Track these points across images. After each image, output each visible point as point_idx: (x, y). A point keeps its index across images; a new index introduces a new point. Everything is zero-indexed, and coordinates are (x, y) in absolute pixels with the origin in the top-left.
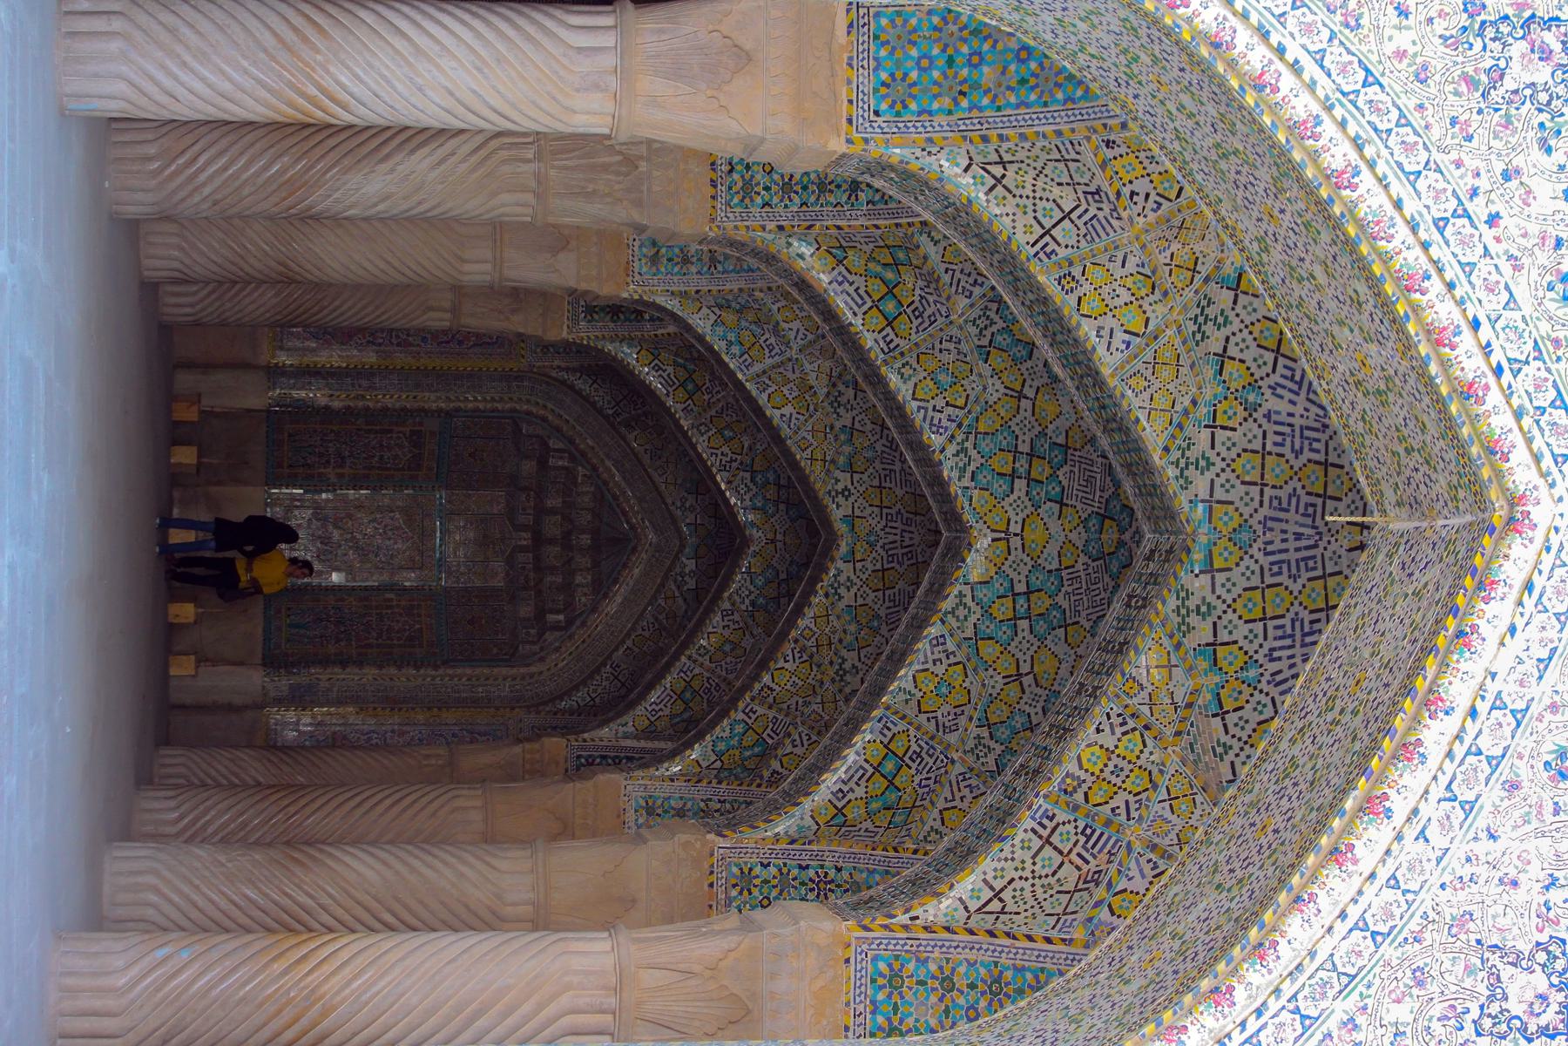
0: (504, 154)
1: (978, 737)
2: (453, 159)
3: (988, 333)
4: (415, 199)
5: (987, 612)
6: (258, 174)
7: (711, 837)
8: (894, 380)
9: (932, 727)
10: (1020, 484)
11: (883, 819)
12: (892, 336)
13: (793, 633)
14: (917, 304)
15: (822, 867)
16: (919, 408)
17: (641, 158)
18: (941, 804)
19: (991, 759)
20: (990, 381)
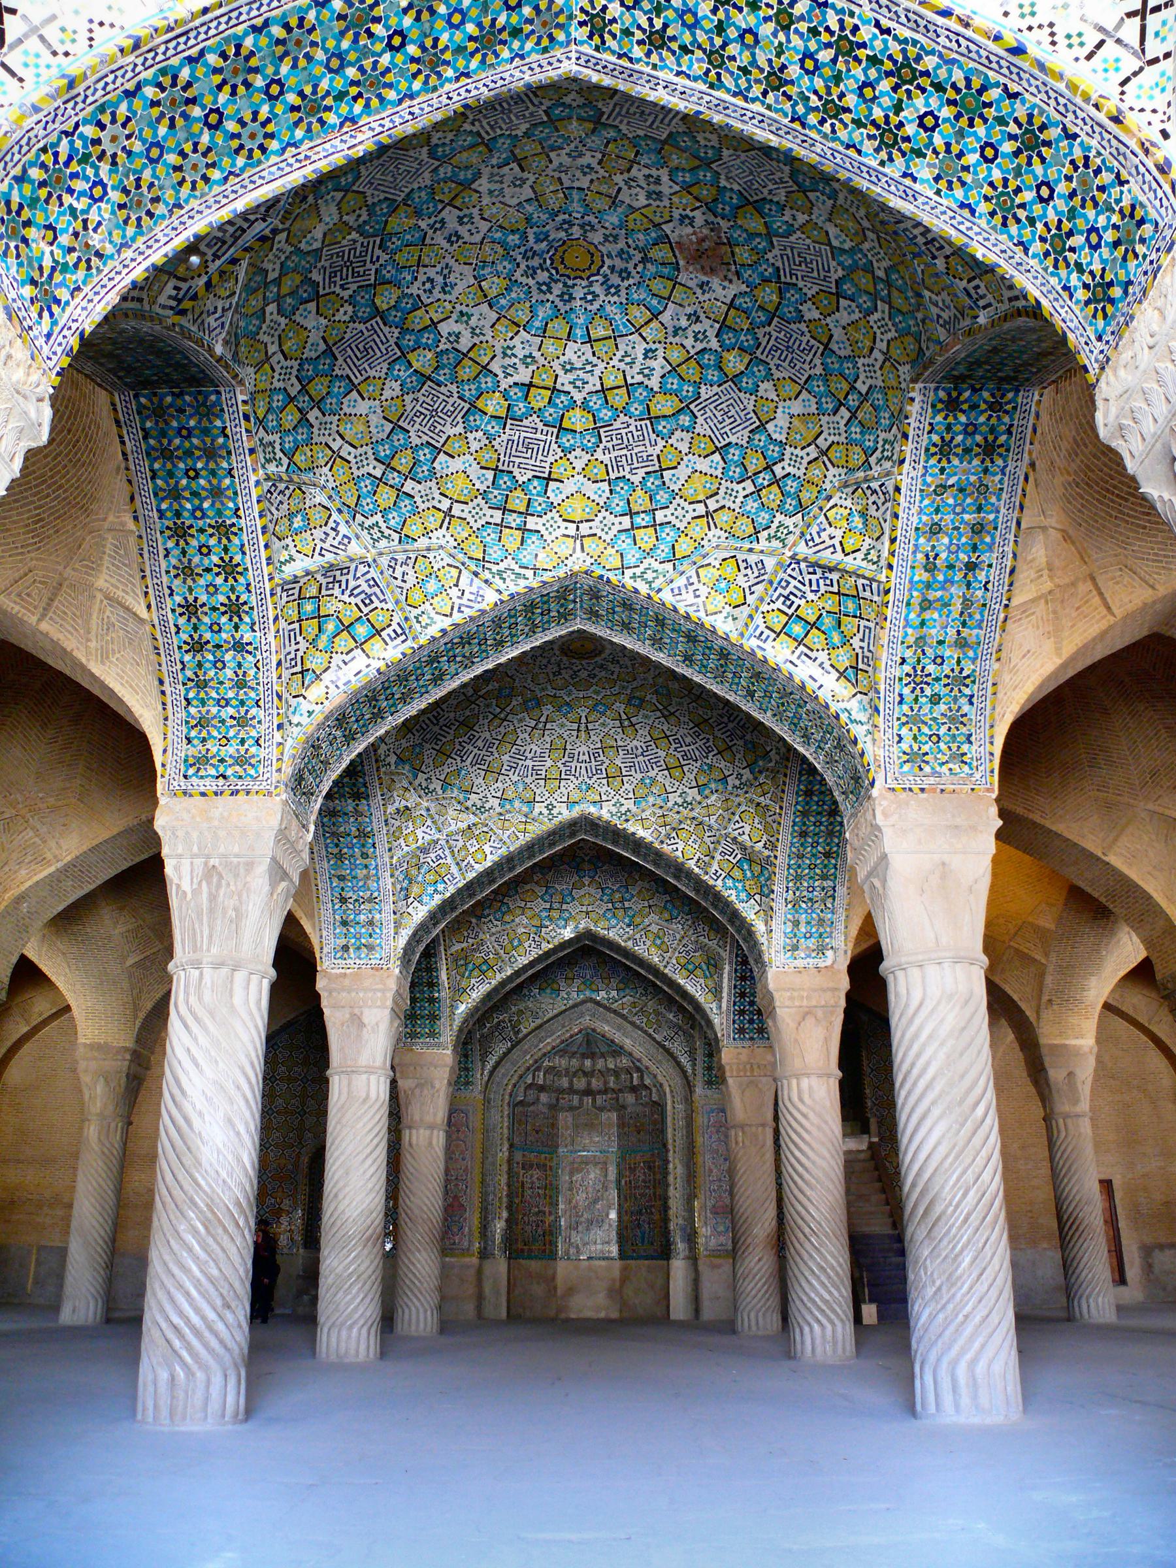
0: (193, 1000)
1: (769, 539)
2: (194, 1050)
3: (387, 532)
4: (233, 1091)
5: (649, 553)
6: (196, 1259)
7: (875, 792)
8: (433, 631)
9: (759, 589)
10: (532, 522)
11: (849, 624)
12: (389, 631)
13: (656, 845)
14: (358, 600)
15: (901, 679)
16: (460, 611)
17: (206, 864)
18: (839, 556)
19: (789, 522)
20: (434, 540)
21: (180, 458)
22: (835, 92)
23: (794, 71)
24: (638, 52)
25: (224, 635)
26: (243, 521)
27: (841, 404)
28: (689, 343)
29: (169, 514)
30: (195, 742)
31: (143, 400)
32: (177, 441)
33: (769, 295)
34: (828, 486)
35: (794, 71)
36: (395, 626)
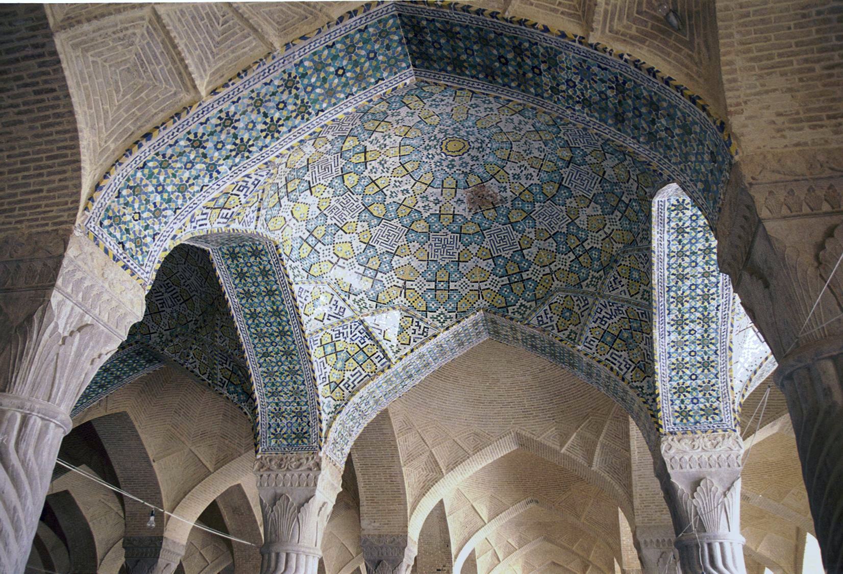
11: (352, 364)
21: (350, 59)
22: (688, 299)
23: (688, 283)
24: (673, 224)
25: (216, 154)
26: (315, 118)
27: (435, 281)
28: (420, 204)
29: (301, 70)
30: (122, 200)
31: (391, 21)
32: (363, 53)
33: (471, 228)
34: (396, 302)
35: (688, 283)
36: (230, 212)
